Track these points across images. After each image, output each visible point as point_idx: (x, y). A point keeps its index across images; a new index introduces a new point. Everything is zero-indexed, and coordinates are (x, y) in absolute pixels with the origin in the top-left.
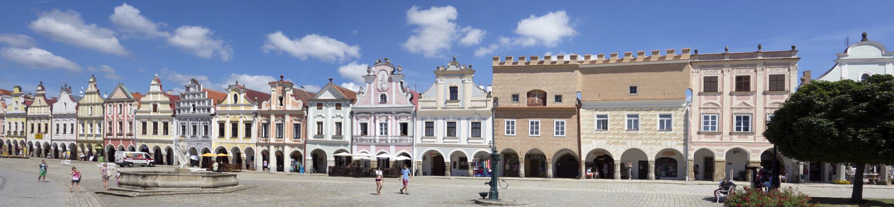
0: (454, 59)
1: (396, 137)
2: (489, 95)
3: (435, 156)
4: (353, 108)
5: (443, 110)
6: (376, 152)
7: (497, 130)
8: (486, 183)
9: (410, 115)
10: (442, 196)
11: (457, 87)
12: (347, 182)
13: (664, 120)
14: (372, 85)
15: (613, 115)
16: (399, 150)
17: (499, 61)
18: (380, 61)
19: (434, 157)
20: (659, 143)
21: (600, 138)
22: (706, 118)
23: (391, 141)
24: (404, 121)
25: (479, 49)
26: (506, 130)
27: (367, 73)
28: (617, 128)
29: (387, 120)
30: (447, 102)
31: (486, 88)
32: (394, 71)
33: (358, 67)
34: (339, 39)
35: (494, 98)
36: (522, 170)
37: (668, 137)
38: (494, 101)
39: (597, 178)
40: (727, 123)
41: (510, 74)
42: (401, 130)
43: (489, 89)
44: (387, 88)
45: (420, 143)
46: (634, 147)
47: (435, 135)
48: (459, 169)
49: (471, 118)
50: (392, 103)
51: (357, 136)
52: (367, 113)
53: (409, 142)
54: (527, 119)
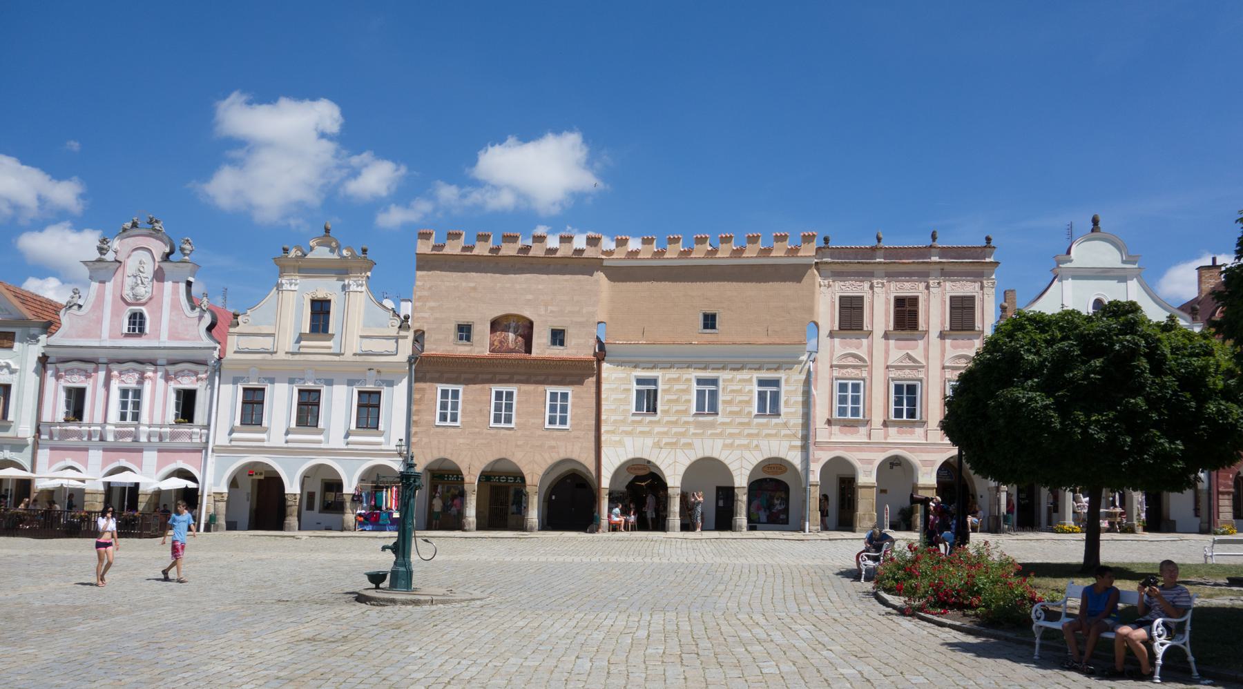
0: (327, 230)
1: (161, 426)
2: (404, 324)
3: (262, 477)
4: (48, 346)
5: (290, 357)
6: (103, 467)
7: (418, 411)
8: (384, 548)
9: (203, 368)
10: (274, 585)
11: (329, 301)
12: (11, 552)
13: (766, 392)
14: (109, 286)
15: (669, 380)
16: (167, 463)
17: (432, 241)
18: (135, 225)
19: (260, 480)
20: (757, 446)
21: (640, 432)
22: (843, 387)
23: (149, 436)
24: (187, 383)
25: (386, 210)
26: (438, 411)
27: (97, 255)
28: (675, 408)
29: (141, 381)
30: (301, 337)
31: (398, 305)
32: (172, 252)
33: (74, 238)
34: (27, 158)
35: (416, 332)
36: (471, 512)
37: (774, 432)
38: (416, 340)
39: (633, 529)
40: (879, 402)
41: (455, 275)
42: (177, 409)
43: (406, 308)
44: (148, 296)
45: (227, 443)
46: (708, 454)
47: (265, 423)
48: (320, 512)
49: (358, 381)
50: (158, 337)
51: (53, 424)
52: (88, 361)
53: (196, 440)
54: (487, 386)
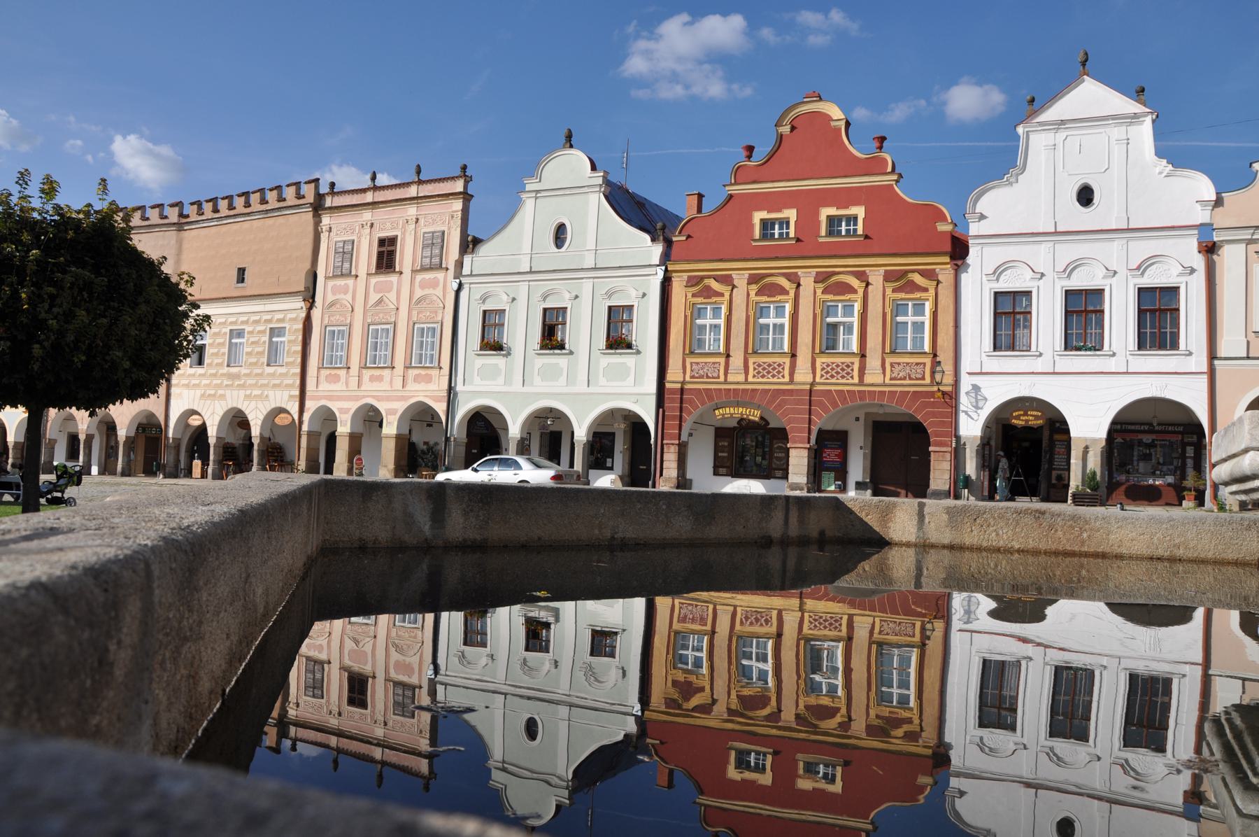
20: (267, 396)
37: (277, 382)
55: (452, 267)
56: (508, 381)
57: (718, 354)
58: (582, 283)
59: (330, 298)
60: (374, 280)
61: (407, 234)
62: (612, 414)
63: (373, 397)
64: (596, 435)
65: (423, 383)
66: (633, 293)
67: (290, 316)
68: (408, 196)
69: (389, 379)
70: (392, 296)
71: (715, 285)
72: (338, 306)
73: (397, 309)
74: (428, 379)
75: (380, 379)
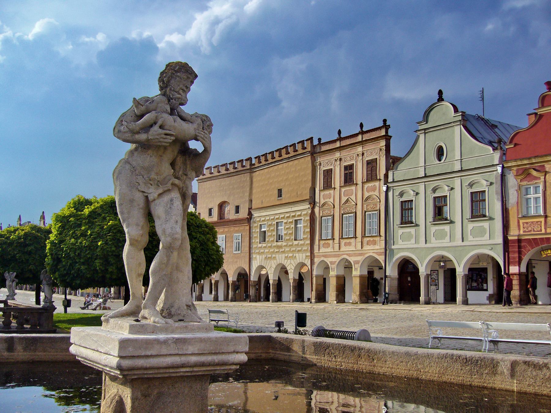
37: (300, 249)
55: (382, 177)
56: (417, 242)
57: (540, 216)
58: (454, 180)
59: (322, 202)
60: (343, 190)
61: (358, 163)
62: (479, 257)
63: (347, 254)
64: (470, 270)
65: (372, 245)
66: (485, 183)
67: (303, 213)
68: (357, 141)
69: (354, 244)
70: (353, 197)
71: (534, 173)
72: (326, 205)
73: (356, 204)
74: (375, 243)
75: (349, 244)
